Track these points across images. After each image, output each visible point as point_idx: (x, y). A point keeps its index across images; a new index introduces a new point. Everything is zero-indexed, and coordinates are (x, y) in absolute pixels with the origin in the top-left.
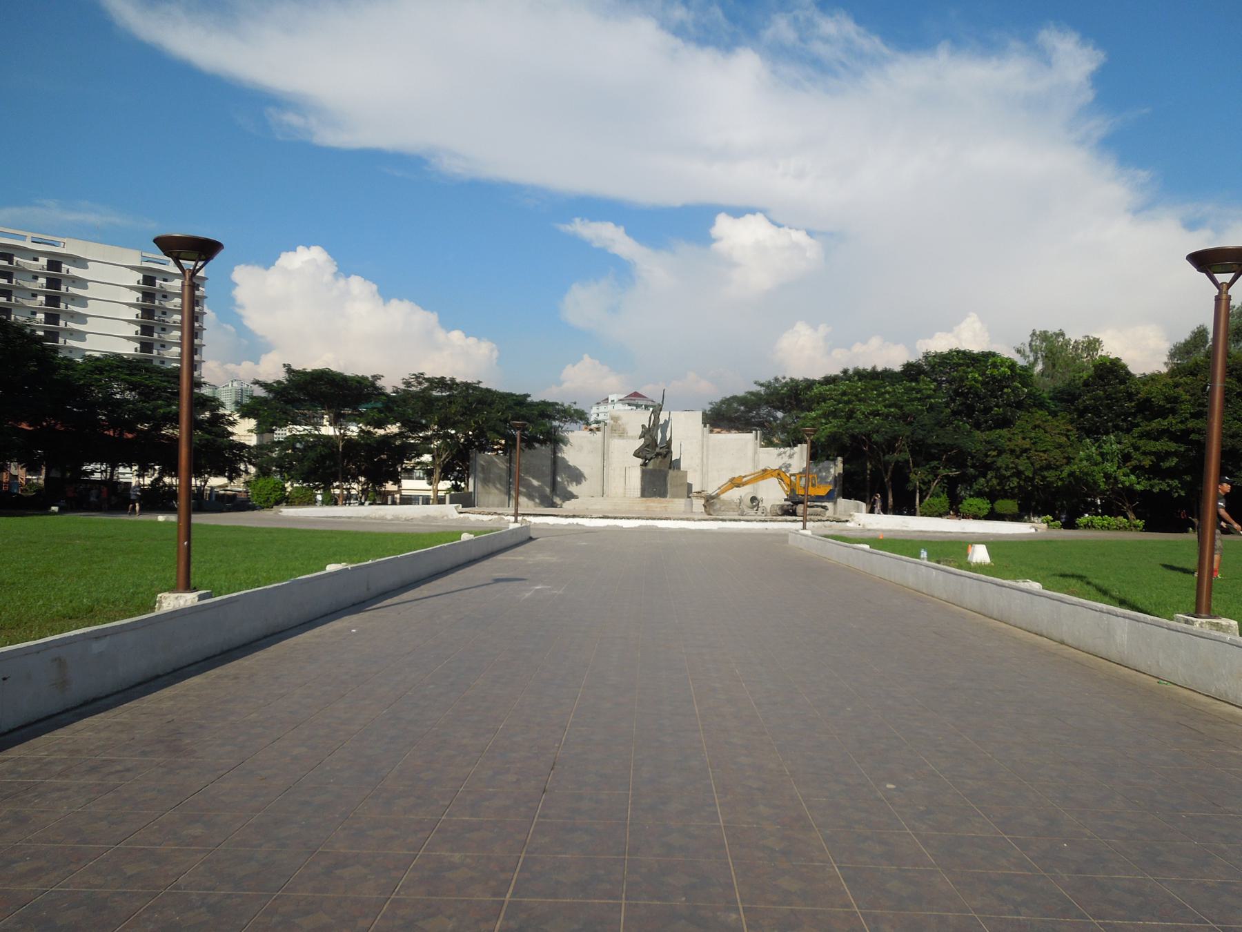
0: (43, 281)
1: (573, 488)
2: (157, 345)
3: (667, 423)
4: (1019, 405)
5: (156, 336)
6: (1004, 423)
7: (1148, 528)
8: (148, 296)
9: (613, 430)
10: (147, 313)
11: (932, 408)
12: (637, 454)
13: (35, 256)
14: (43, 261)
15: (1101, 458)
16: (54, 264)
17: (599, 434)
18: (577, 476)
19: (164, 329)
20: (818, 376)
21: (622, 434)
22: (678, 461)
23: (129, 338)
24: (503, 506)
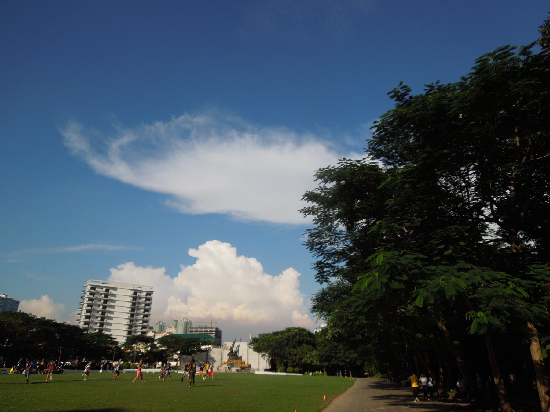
0: (103, 295)
2: (135, 315)
3: (238, 346)
4: (300, 343)
6: (294, 347)
7: (328, 375)
8: (135, 298)
9: (225, 348)
10: (134, 304)
11: (277, 343)
12: (228, 355)
13: (102, 288)
14: (104, 289)
15: (311, 357)
16: (107, 290)
17: (221, 349)
20: (271, 332)
21: (227, 349)
22: (241, 357)
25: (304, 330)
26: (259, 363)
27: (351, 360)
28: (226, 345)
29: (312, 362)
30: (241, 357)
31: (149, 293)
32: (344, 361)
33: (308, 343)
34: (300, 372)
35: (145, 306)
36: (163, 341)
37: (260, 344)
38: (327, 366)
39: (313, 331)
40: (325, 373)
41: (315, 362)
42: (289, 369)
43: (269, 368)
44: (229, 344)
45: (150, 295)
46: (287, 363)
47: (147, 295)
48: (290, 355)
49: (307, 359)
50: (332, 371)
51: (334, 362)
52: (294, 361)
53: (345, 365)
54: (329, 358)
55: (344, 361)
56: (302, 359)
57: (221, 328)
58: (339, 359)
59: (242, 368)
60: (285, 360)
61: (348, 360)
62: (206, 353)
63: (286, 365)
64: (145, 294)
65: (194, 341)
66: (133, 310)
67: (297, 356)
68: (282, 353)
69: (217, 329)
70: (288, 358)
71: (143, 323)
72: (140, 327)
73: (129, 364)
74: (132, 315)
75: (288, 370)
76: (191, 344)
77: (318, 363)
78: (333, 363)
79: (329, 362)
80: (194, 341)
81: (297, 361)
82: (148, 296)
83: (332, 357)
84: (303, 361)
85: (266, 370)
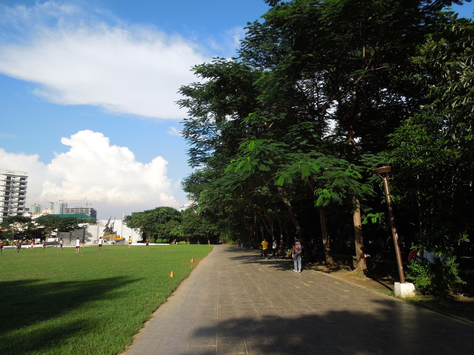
1: (89, 238)
3: (113, 223)
4: (168, 219)
5: (10, 195)
6: (163, 223)
7: (191, 244)
8: (8, 183)
9: (100, 225)
10: (8, 188)
11: (148, 219)
12: (104, 231)
15: (178, 230)
18: (91, 236)
19: (13, 193)
21: (102, 226)
22: (116, 232)
23: (1, 196)
24: (68, 244)
25: (172, 209)
26: (133, 236)
27: (210, 231)
28: (101, 222)
29: (178, 234)
30: (116, 232)
31: (23, 178)
32: (204, 232)
33: (175, 219)
34: (167, 243)
35: (20, 190)
36: (40, 220)
37: (132, 221)
38: (190, 237)
39: (180, 210)
40: (188, 243)
41: (180, 234)
42: (158, 240)
43: (141, 239)
44: (105, 222)
45: (24, 179)
46: (157, 235)
47: (21, 179)
48: (159, 229)
49: (173, 232)
50: (193, 241)
51: (195, 234)
52: (163, 234)
53: (205, 236)
54: (192, 231)
55: (204, 232)
56: (169, 232)
57: (95, 209)
58: (200, 232)
59: (117, 241)
60: (155, 234)
61: (208, 232)
62: (83, 230)
63: (156, 237)
64: (19, 178)
65: (71, 220)
66: (7, 193)
67: (166, 230)
68: (152, 228)
69: (92, 209)
70: (157, 232)
71: (18, 205)
72: (17, 209)
73: (7, 242)
74: (7, 198)
75: (157, 241)
76: (69, 223)
77: (183, 235)
78: (195, 234)
79: (192, 233)
80: (71, 220)
81: (165, 233)
82: (22, 181)
83: (195, 230)
84: (170, 233)
85: (138, 242)
